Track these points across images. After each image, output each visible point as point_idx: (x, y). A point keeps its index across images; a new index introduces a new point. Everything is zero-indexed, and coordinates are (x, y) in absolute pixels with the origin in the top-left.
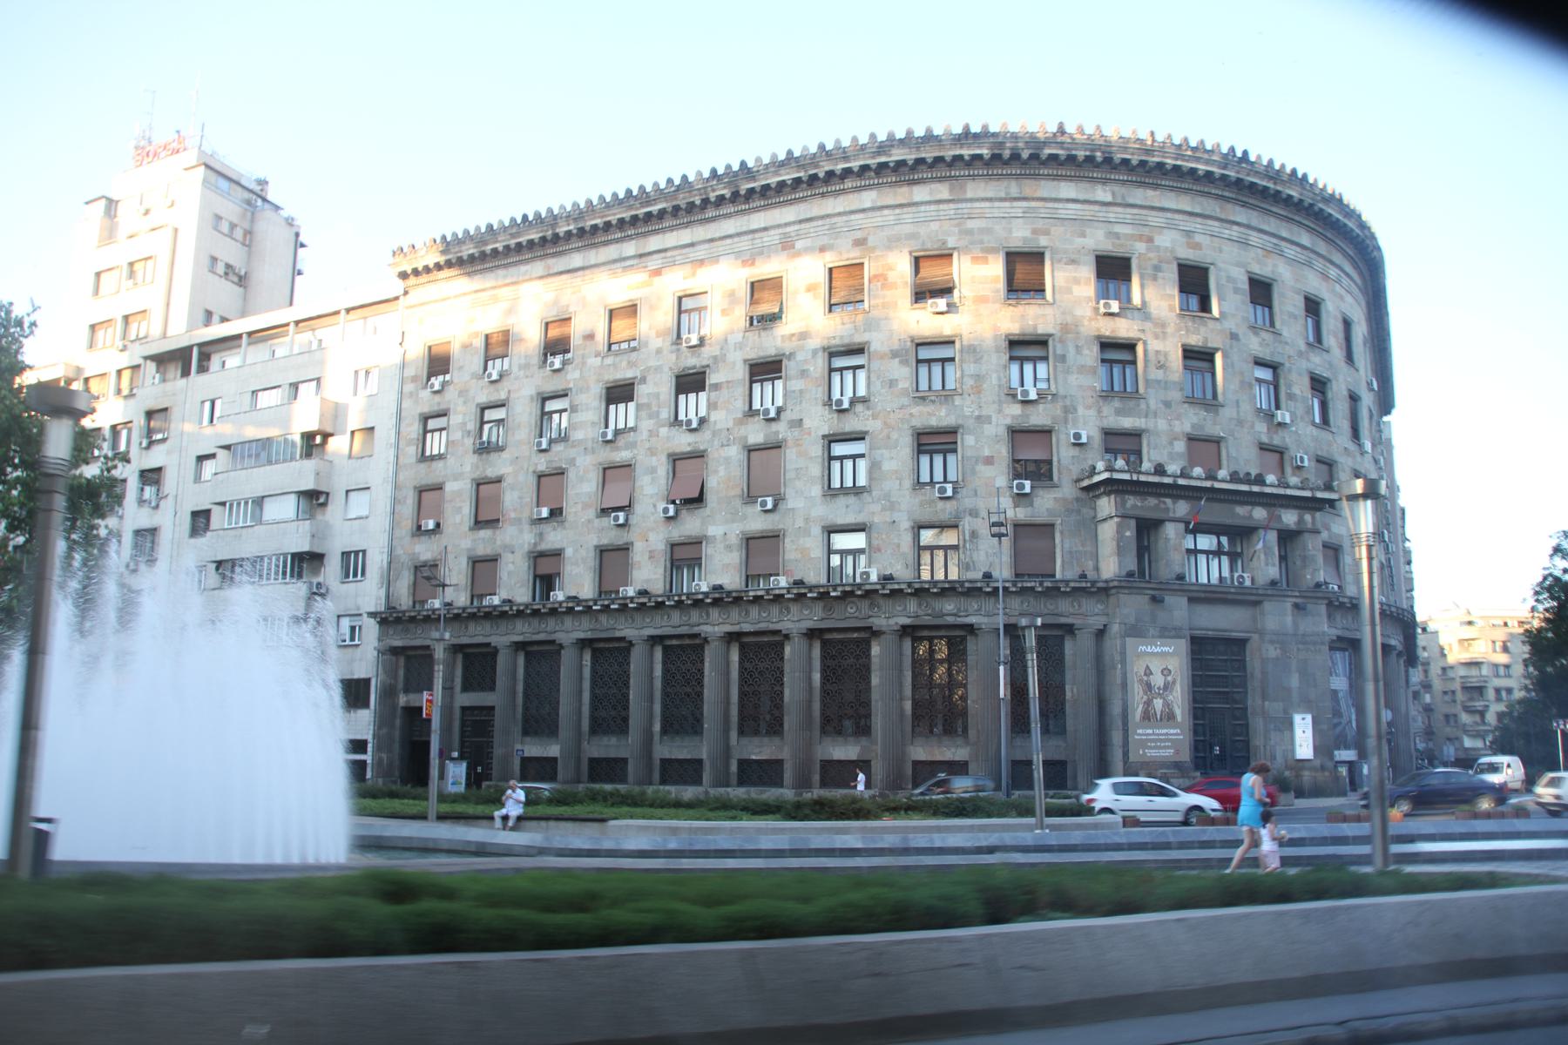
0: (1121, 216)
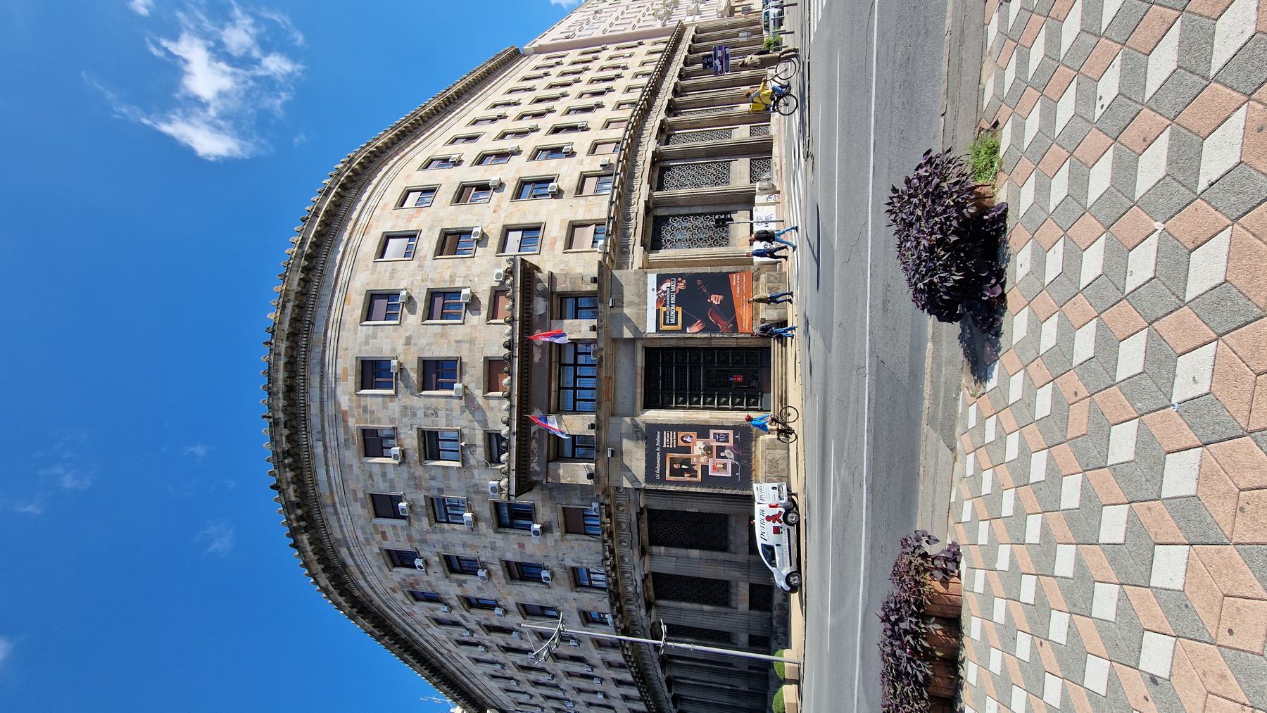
0: (332, 436)
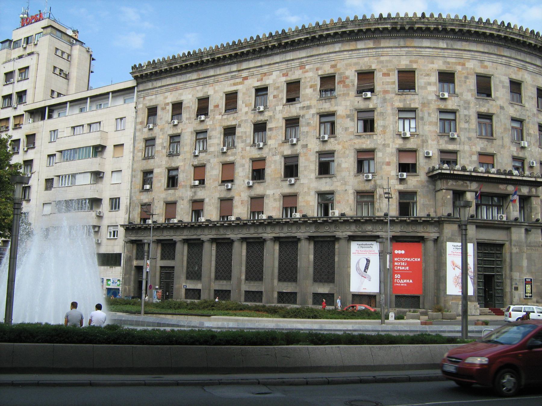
0: (450, 54)
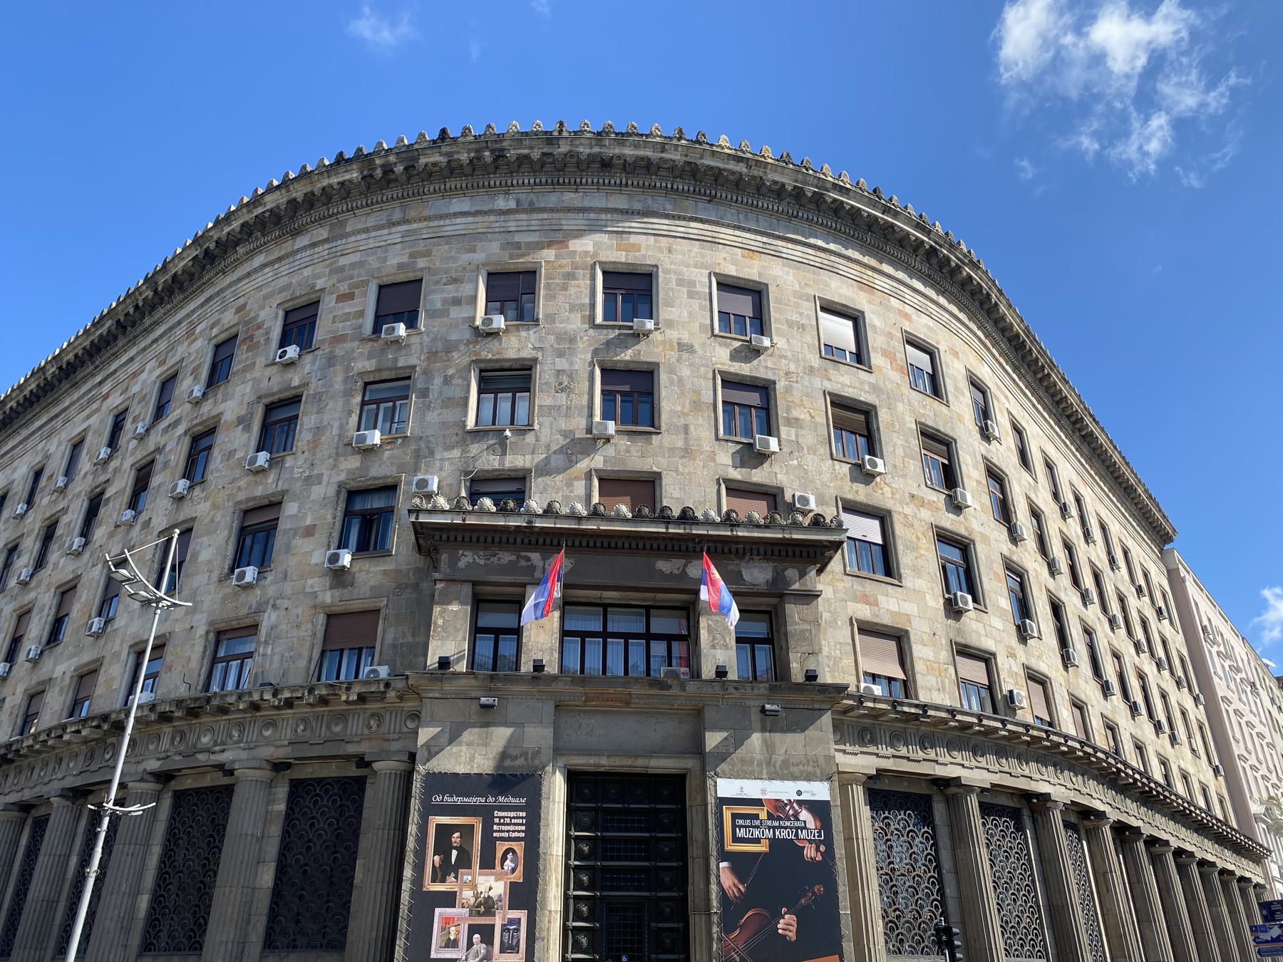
0: (525, 223)
